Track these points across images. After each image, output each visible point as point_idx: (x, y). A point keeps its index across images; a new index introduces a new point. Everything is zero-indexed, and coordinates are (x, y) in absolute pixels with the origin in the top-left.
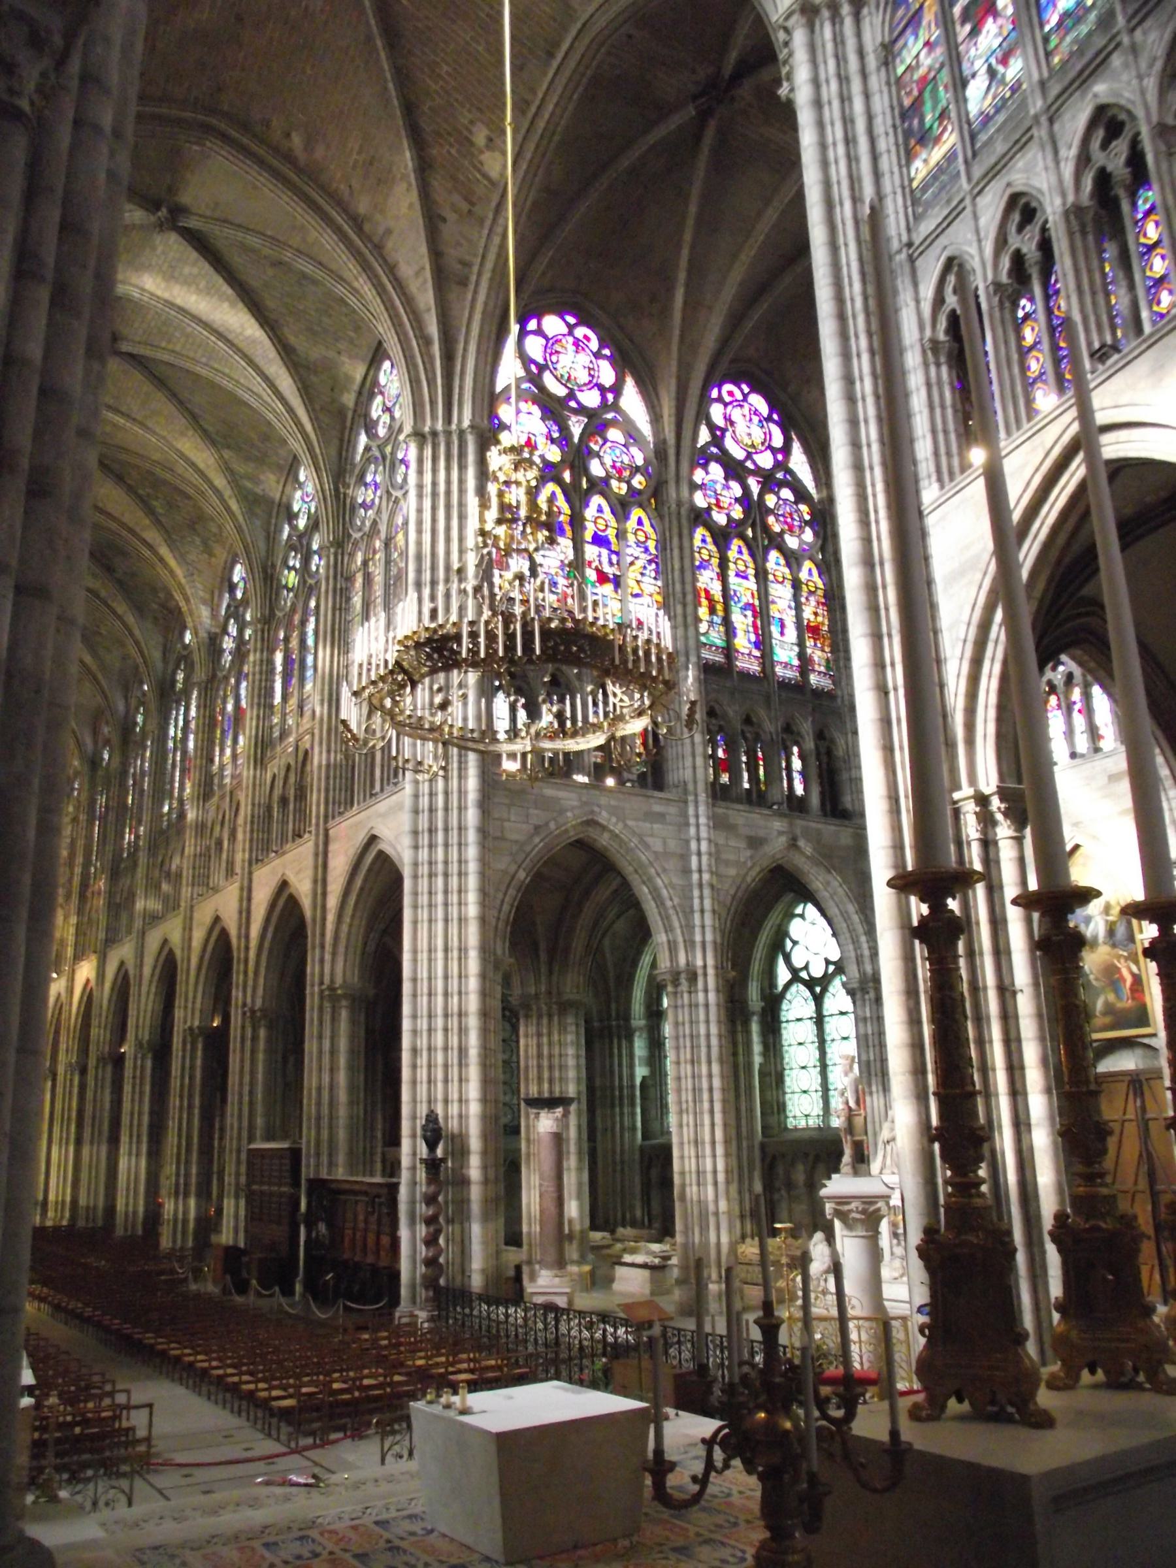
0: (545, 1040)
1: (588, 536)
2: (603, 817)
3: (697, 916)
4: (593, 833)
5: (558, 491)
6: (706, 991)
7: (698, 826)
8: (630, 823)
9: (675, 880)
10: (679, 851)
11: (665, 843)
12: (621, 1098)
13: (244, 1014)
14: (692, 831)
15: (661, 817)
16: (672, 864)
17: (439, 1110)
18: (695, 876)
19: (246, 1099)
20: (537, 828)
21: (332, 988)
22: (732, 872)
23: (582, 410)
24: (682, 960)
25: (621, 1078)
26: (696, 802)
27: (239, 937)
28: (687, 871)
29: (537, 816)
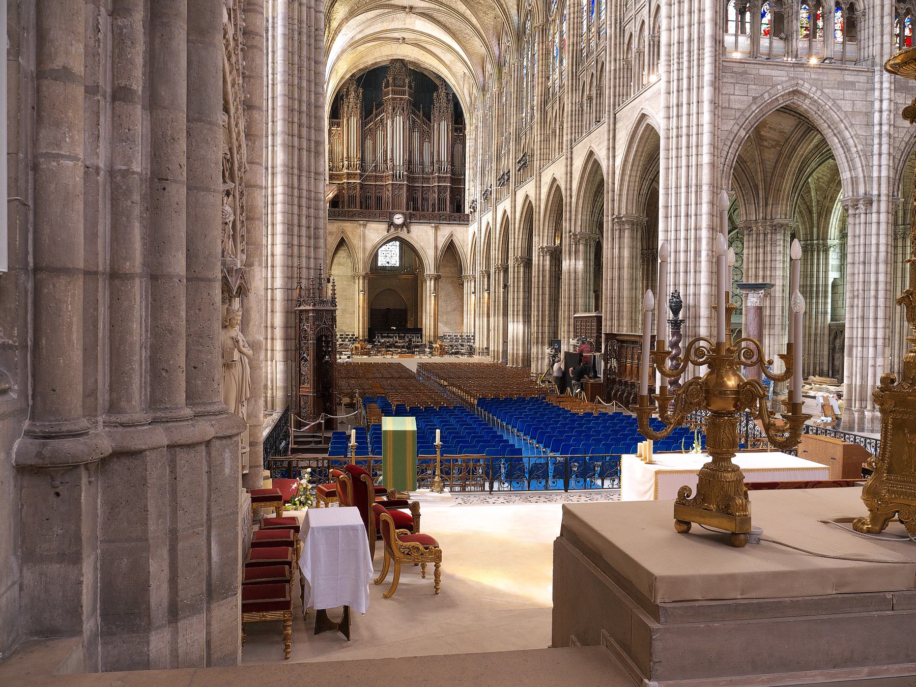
0: (761, 250)
2: (805, 88)
3: (876, 158)
6: (879, 212)
7: (881, 89)
8: (826, 91)
12: (817, 292)
13: (570, 237)
14: (877, 93)
17: (682, 291)
18: (877, 128)
19: (572, 287)
20: (755, 98)
21: (618, 218)
24: (862, 191)
25: (818, 278)
27: (566, 189)
28: (869, 125)
29: (755, 90)
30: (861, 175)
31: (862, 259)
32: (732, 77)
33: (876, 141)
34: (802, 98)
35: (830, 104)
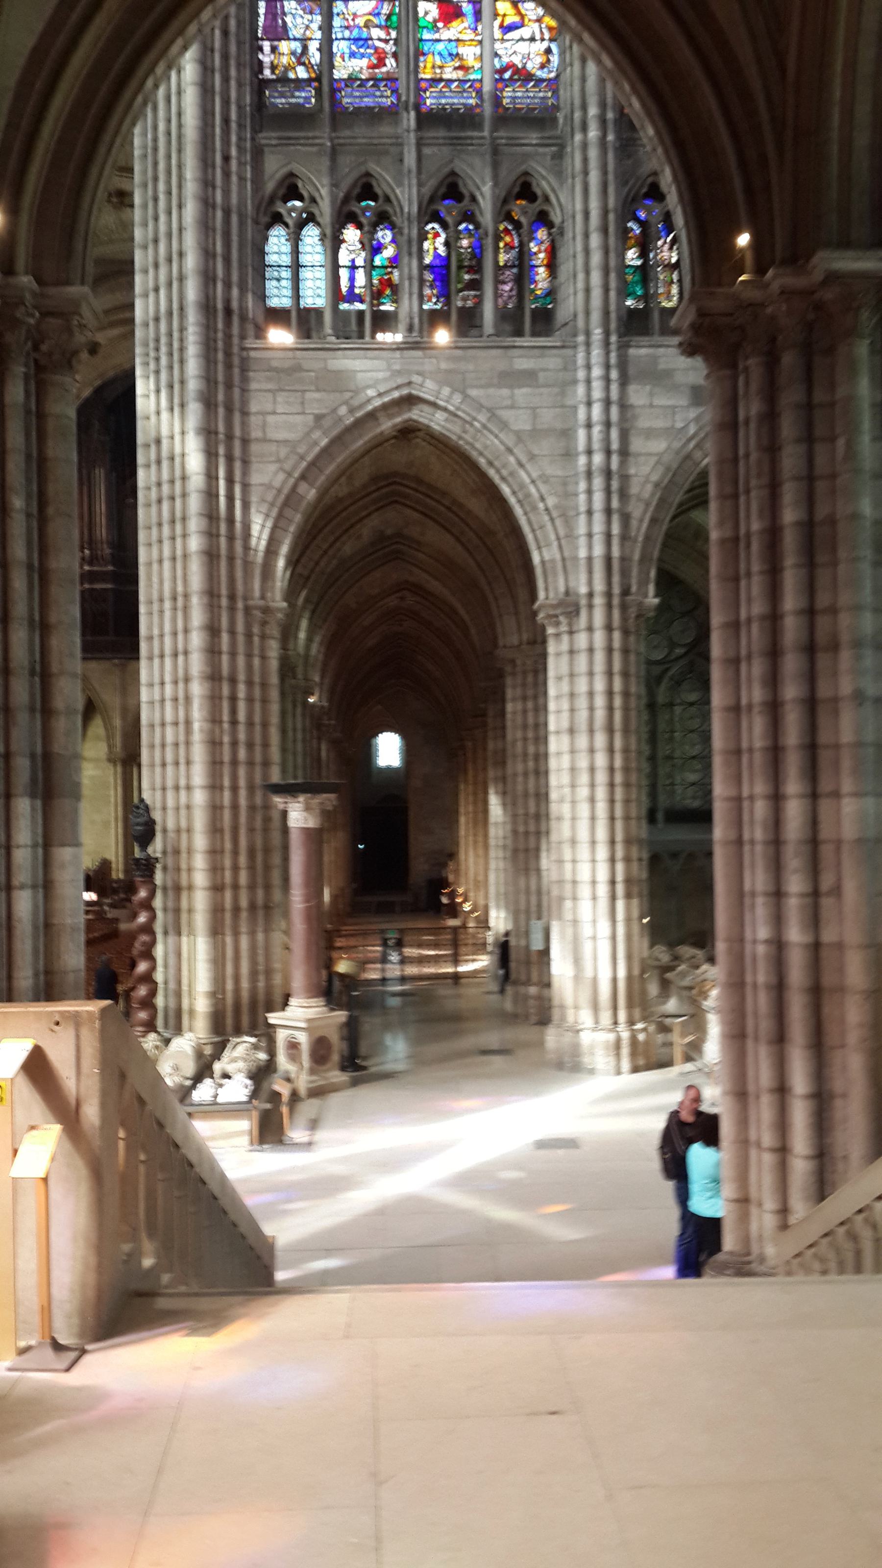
2: (428, 389)
3: (582, 519)
4: (417, 414)
6: (590, 629)
7: (588, 381)
8: (473, 392)
9: (550, 471)
10: (559, 425)
11: (535, 417)
15: (529, 377)
16: (545, 447)
18: (582, 460)
20: (319, 418)
22: (659, 446)
26: (588, 344)
28: (569, 455)
29: (317, 401)
30: (558, 557)
31: (565, 724)
32: (269, 379)
33: (582, 486)
34: (427, 408)
35: (482, 417)
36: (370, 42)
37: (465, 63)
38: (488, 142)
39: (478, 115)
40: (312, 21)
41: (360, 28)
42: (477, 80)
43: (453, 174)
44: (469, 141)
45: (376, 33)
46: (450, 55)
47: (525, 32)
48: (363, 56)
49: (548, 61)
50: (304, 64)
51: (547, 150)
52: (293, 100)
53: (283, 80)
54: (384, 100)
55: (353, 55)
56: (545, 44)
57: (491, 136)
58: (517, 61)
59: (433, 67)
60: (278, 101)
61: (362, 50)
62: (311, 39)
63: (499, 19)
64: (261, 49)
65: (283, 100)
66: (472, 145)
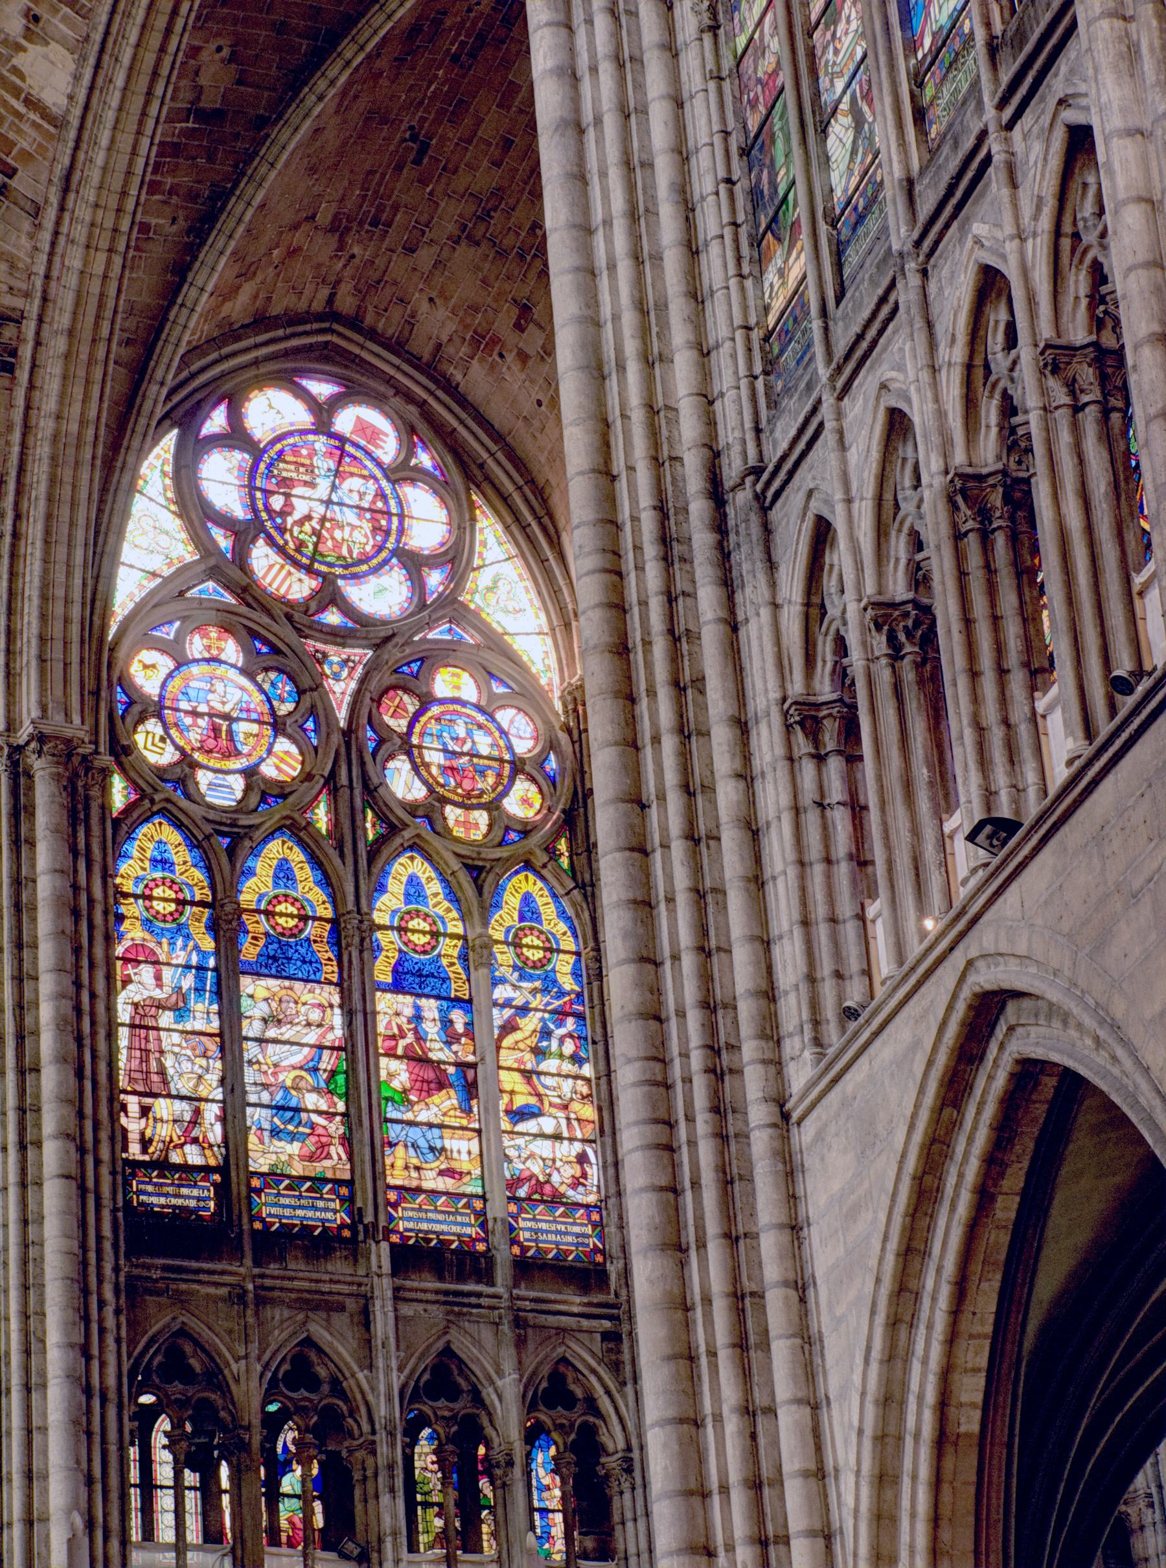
1: (382, 971)
5: (297, 856)
23: (361, 628)
36: (304, 1115)
37: (455, 1165)
38: (505, 1304)
39: (484, 1254)
40: (207, 1070)
41: (286, 1089)
42: (477, 1196)
43: (447, 1352)
44: (473, 1300)
45: (312, 1100)
46: (432, 1149)
47: (547, 1124)
48: (293, 1137)
49: (584, 1175)
50: (195, 1141)
51: (594, 1323)
52: (179, 1202)
53: (163, 1166)
54: (329, 1215)
55: (275, 1133)
56: (577, 1147)
57: (512, 1298)
58: (536, 1168)
59: (407, 1168)
60: (154, 1200)
61: (290, 1127)
62: (207, 1100)
63: (506, 1098)
64: (124, 1107)
65: (162, 1200)
66: (479, 1306)
